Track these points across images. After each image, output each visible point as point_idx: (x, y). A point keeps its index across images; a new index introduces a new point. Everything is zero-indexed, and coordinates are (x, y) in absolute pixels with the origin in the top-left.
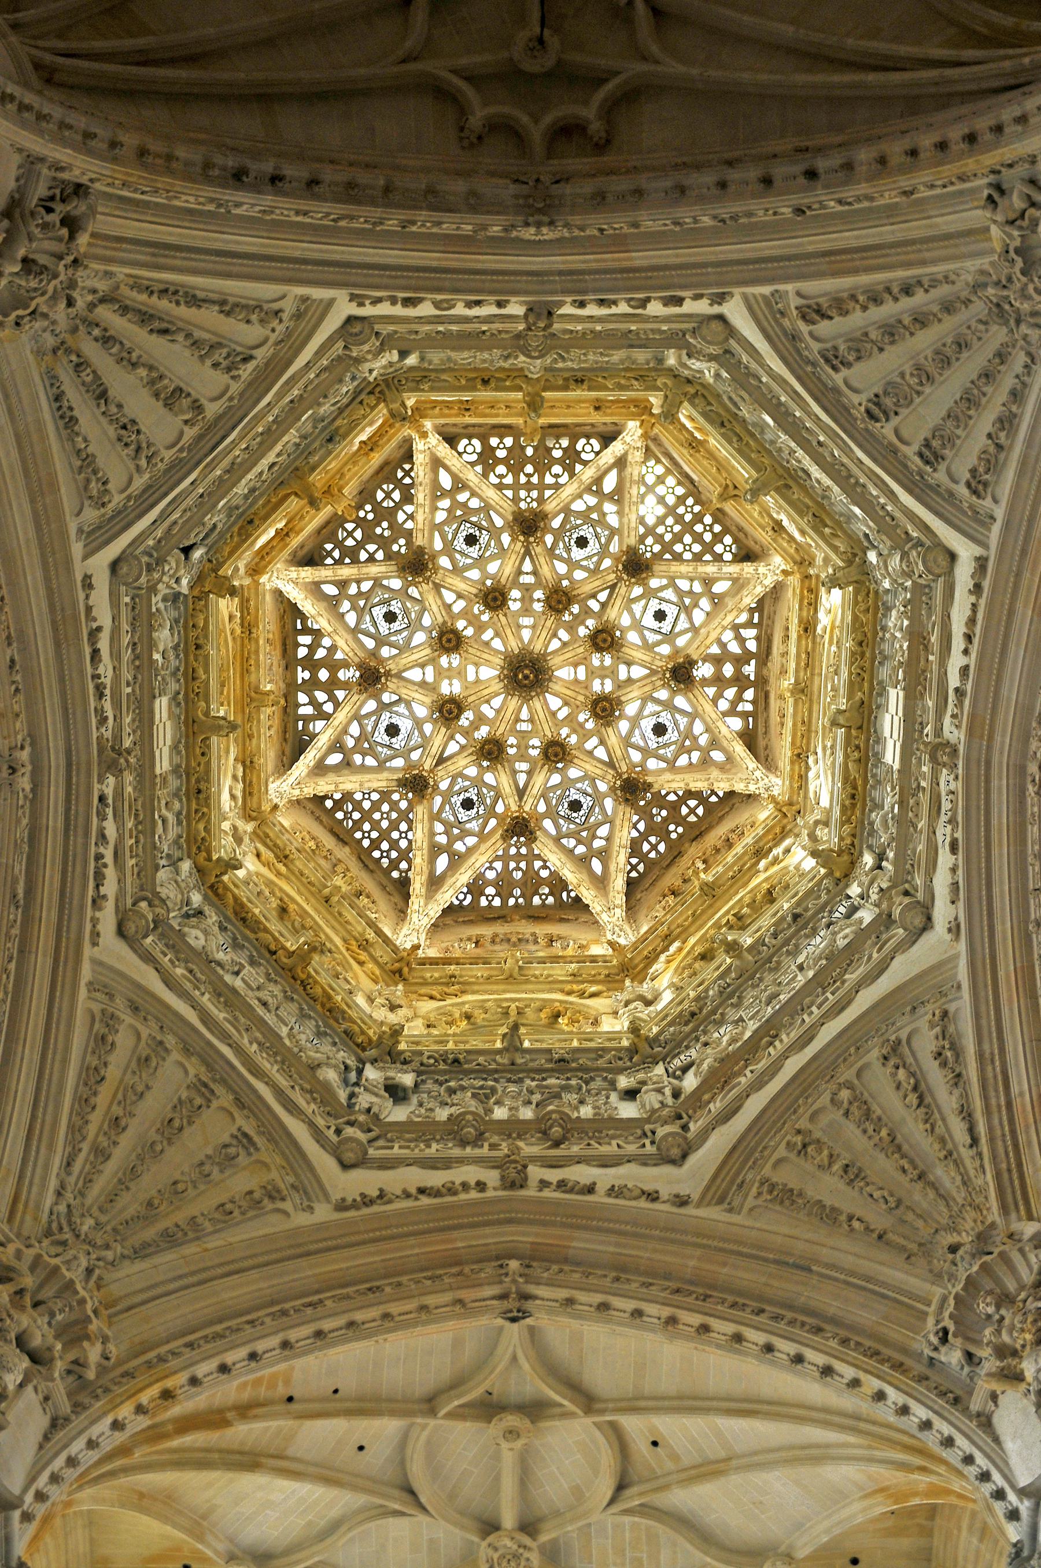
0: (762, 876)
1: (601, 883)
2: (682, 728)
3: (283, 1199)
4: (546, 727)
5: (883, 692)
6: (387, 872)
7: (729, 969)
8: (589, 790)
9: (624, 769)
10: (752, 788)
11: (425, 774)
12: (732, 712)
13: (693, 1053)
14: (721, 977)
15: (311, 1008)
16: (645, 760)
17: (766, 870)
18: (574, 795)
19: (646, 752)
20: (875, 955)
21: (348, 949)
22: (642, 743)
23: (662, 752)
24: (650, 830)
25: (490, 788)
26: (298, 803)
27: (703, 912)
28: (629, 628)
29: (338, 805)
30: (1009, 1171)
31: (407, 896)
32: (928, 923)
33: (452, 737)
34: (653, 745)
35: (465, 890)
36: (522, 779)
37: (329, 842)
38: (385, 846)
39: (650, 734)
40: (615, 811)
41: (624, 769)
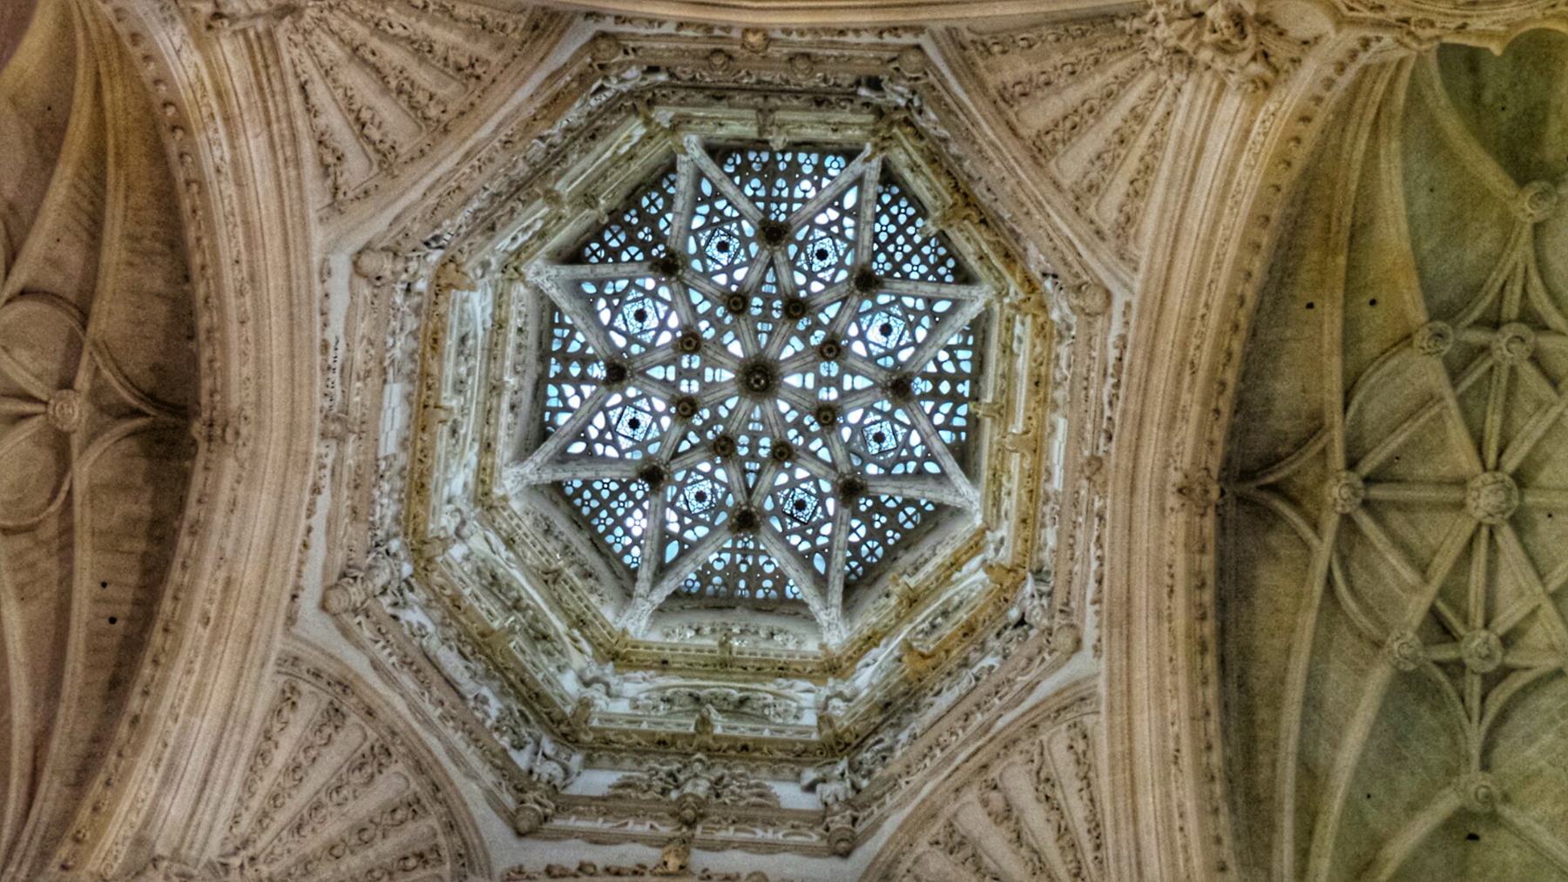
1: (700, 175)
3: (973, 42)
5: (403, 443)
6: (903, 193)
7: (557, 179)
8: (709, 262)
13: (593, 102)
14: (565, 171)
15: (950, 165)
18: (724, 258)
22: (658, 304)
24: (653, 221)
25: (800, 270)
27: (596, 181)
28: (662, 414)
29: (942, 261)
30: (267, 67)
33: (832, 321)
34: (648, 301)
36: (770, 277)
38: (902, 219)
39: (650, 312)
40: (686, 244)
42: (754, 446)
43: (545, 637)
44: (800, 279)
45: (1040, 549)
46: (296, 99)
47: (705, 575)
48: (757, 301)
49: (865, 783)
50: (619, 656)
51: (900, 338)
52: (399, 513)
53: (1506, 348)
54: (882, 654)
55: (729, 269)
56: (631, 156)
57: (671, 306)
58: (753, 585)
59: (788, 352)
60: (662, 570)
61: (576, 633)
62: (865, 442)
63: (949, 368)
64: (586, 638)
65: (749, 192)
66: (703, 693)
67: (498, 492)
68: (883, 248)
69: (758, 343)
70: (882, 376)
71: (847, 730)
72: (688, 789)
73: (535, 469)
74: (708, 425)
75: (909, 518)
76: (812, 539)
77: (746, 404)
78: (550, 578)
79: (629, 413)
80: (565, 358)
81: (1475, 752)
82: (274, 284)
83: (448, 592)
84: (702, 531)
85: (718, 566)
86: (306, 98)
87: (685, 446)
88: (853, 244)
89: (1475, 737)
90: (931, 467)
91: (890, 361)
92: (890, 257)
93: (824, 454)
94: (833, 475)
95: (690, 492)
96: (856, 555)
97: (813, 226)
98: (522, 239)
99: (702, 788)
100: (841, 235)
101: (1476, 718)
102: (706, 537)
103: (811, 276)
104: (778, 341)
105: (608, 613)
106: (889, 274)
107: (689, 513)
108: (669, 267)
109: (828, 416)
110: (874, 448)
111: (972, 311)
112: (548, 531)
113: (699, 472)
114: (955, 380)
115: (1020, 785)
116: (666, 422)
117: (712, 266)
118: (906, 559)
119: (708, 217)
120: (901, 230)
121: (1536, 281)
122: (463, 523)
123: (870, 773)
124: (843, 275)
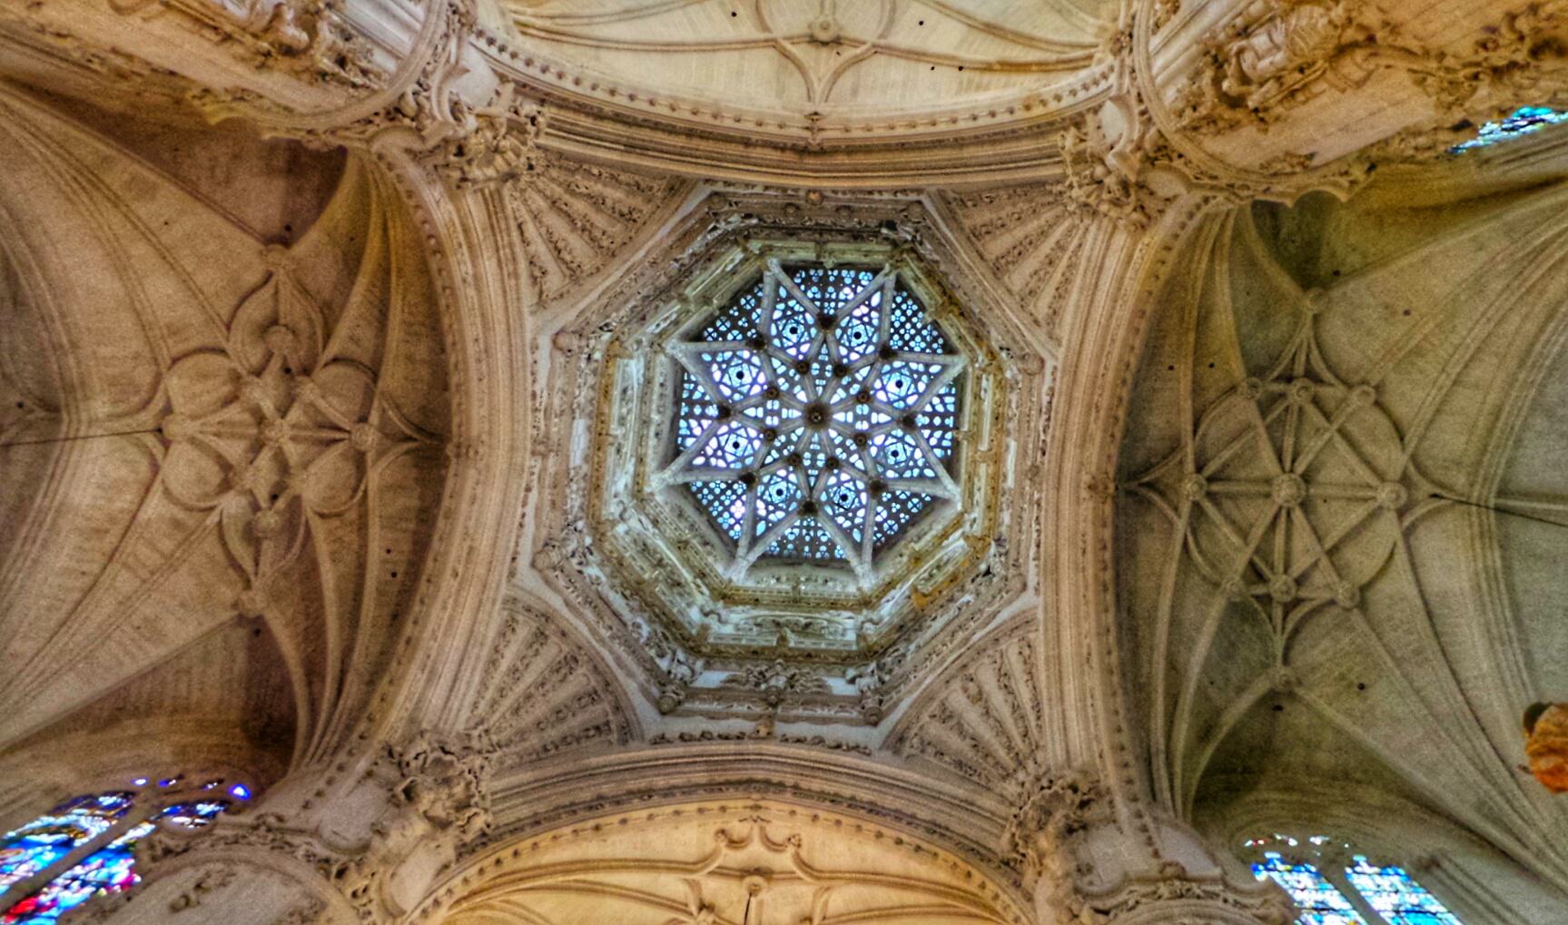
1: (778, 284)
5: (586, 459)
6: (909, 296)
13: (709, 237)
18: (794, 338)
24: (748, 314)
29: (935, 340)
36: (824, 350)
38: (909, 313)
42: (814, 460)
43: (679, 584)
44: (843, 351)
46: (515, 234)
47: (782, 544)
48: (815, 366)
49: (887, 678)
50: (727, 596)
53: (1296, 394)
54: (898, 594)
56: (734, 272)
57: (760, 369)
58: (814, 549)
59: (835, 399)
60: (754, 541)
62: (886, 457)
63: (940, 408)
65: (810, 295)
66: (782, 620)
67: (647, 490)
68: (897, 331)
70: (897, 414)
72: (773, 682)
73: (672, 474)
74: (784, 446)
76: (852, 520)
77: (809, 432)
78: (681, 545)
79: (733, 438)
80: (691, 403)
81: (1279, 653)
82: (501, 354)
84: (780, 514)
85: (791, 538)
86: (522, 233)
87: (769, 459)
88: (877, 329)
89: (1279, 643)
90: (929, 473)
91: (902, 404)
92: (902, 337)
93: (860, 465)
95: (773, 490)
96: (881, 530)
97: (852, 317)
98: (663, 325)
99: (781, 682)
100: (870, 323)
101: (1279, 628)
103: (851, 349)
105: (719, 568)
106: (901, 348)
107: (772, 503)
108: (759, 343)
109: (862, 439)
110: (891, 460)
111: (954, 372)
112: (680, 515)
114: (944, 416)
115: (987, 678)
116: (757, 444)
117: (787, 343)
118: (913, 532)
119: (784, 311)
120: (909, 319)
121: (1315, 352)
122: (625, 510)
123: (890, 671)
124: (871, 349)
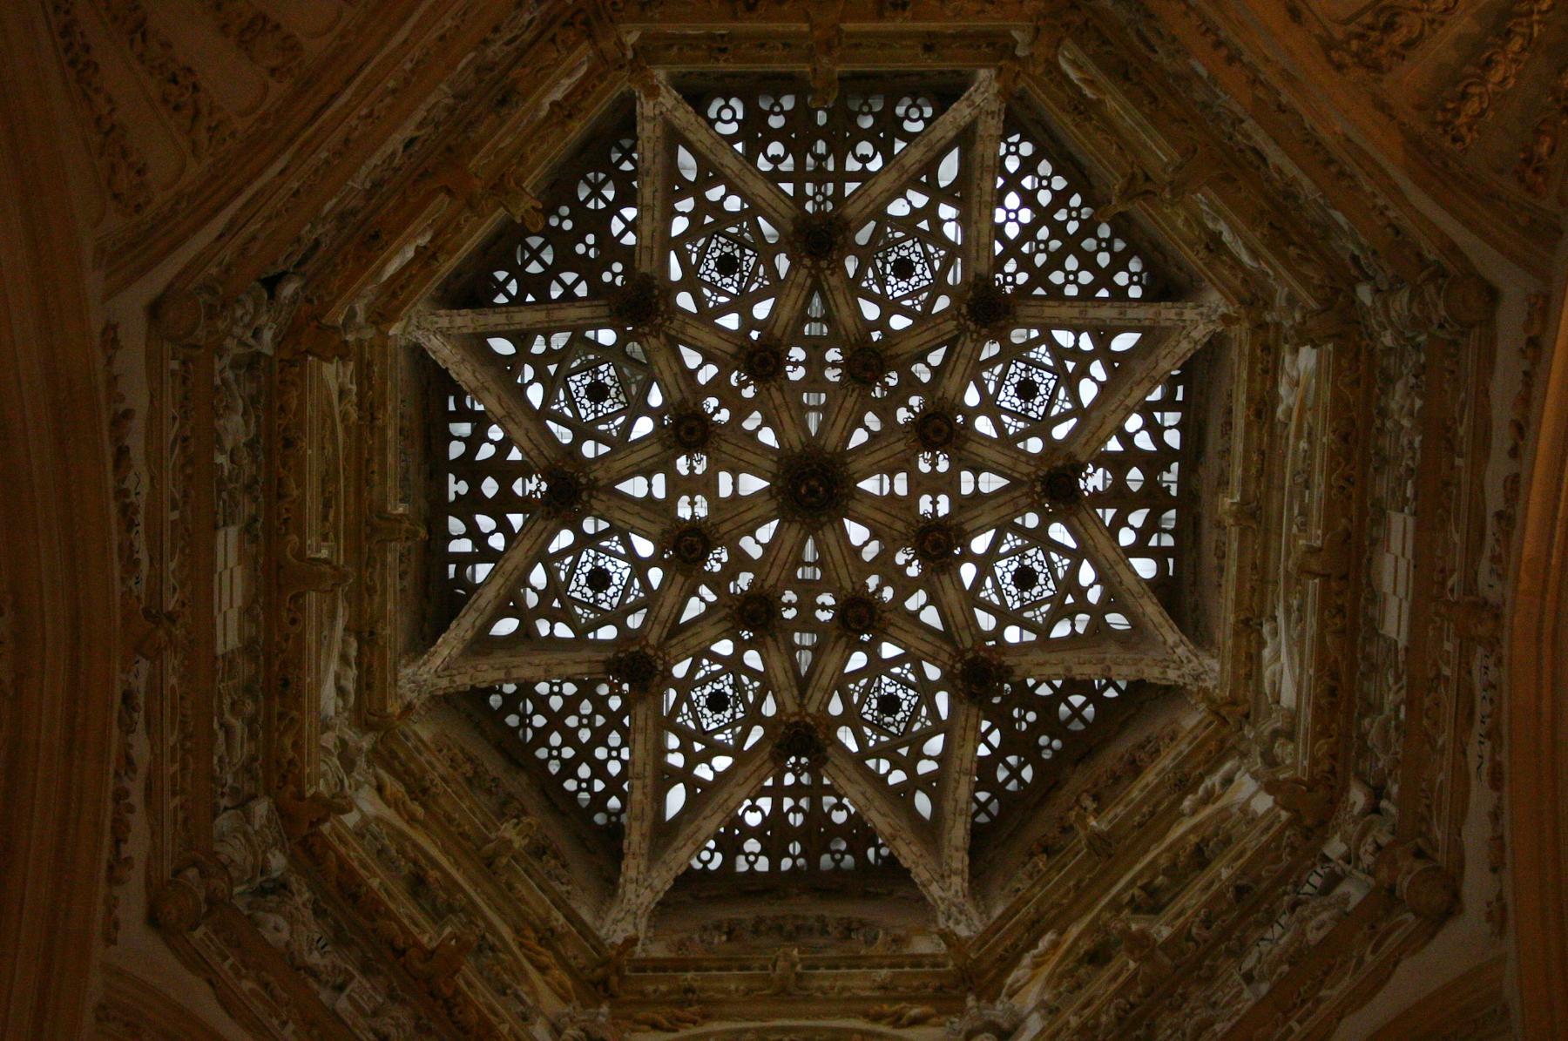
0: (1188, 824)
1: (930, 832)
2: (1061, 573)
4: (843, 573)
7: (1133, 978)
9: (968, 643)
10: (1172, 675)
11: (650, 652)
12: (1139, 549)
14: (1119, 993)
16: (1000, 629)
17: (1194, 812)
19: (1005, 616)
20: (1369, 958)
21: (521, 946)
23: (1028, 614)
26: (445, 702)
29: (511, 703)
31: (618, 856)
32: (1452, 907)
35: (711, 844)
36: (805, 659)
37: (493, 765)
38: (584, 771)
41: (968, 643)
42: (815, 364)
44: (753, 659)
45: (253, 400)
51: (573, 567)
52: (1383, 392)
55: (877, 666)
57: (972, 598)
59: (766, 533)
61: (1088, 92)
63: (485, 522)
64: (1071, 83)
69: (818, 547)
71: (571, 49)
74: (898, 397)
75: (536, 255)
76: (703, 206)
79: (1037, 409)
80: (1153, 497)
83: (1293, 251)
84: (898, 208)
85: (865, 148)
87: (936, 358)
88: (669, 724)
92: (600, 705)
94: (674, 328)
95: (922, 275)
97: (735, 751)
100: (686, 737)
102: (890, 200)
103: (733, 664)
104: (783, 554)
107: (923, 238)
110: (606, 373)
113: (907, 312)
114: (471, 504)
